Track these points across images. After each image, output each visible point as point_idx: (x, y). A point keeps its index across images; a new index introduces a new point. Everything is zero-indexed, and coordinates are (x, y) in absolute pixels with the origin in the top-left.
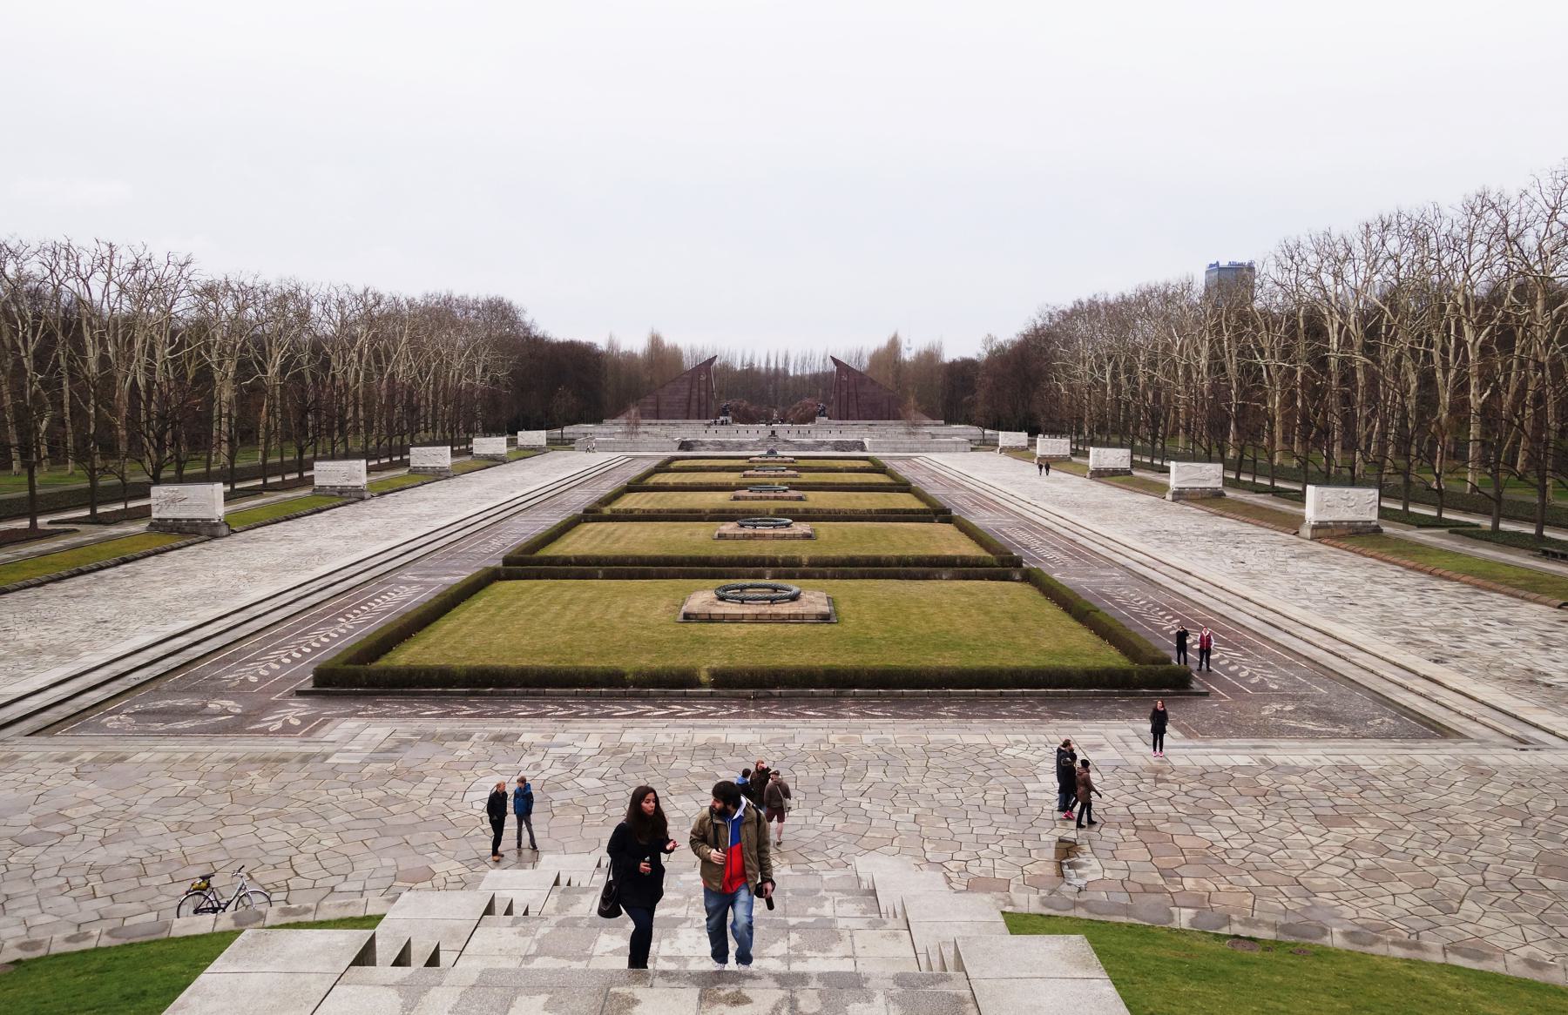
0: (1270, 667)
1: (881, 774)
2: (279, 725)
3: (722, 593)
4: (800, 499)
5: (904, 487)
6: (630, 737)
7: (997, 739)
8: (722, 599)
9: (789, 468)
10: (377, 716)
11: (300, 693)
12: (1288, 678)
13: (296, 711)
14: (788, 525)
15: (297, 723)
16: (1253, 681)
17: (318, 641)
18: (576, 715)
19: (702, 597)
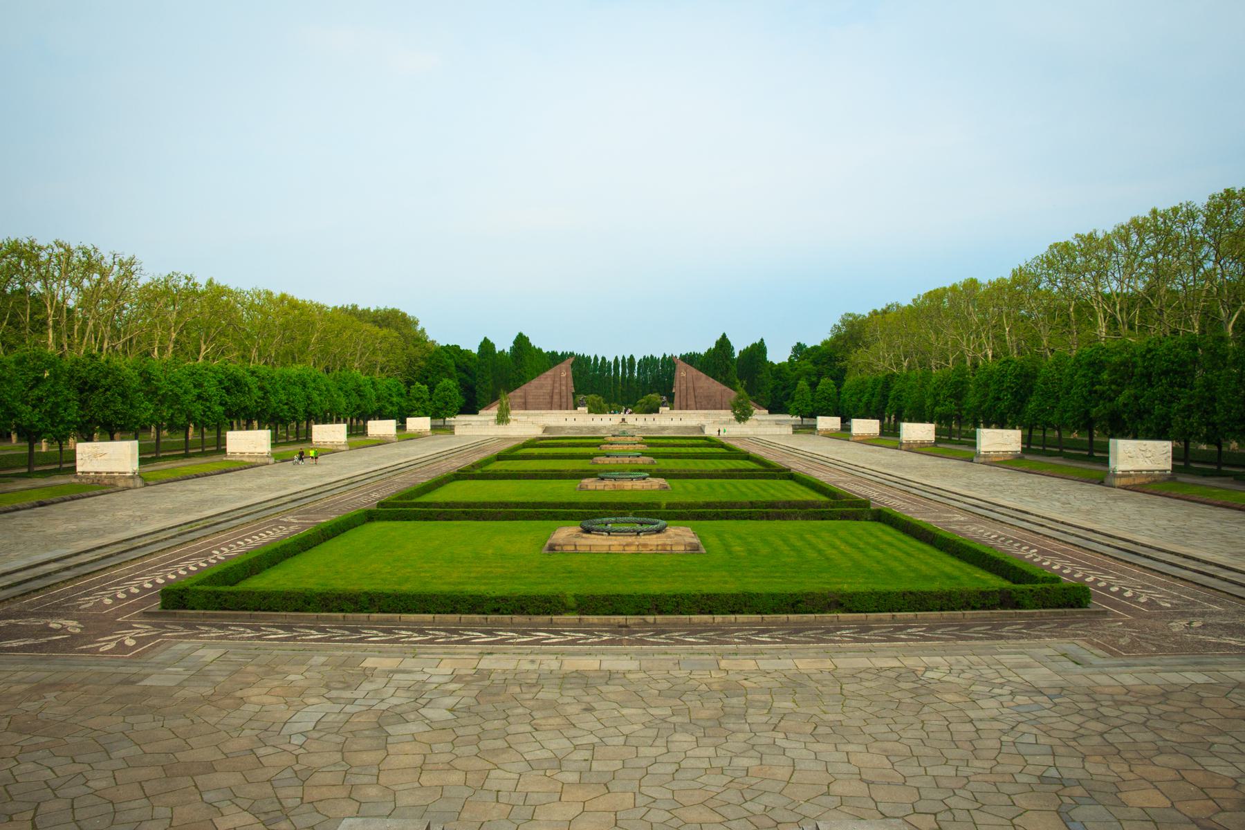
1: (792, 705)
7: (910, 662)
8: (588, 531)
12: (1174, 597)
19: (565, 533)
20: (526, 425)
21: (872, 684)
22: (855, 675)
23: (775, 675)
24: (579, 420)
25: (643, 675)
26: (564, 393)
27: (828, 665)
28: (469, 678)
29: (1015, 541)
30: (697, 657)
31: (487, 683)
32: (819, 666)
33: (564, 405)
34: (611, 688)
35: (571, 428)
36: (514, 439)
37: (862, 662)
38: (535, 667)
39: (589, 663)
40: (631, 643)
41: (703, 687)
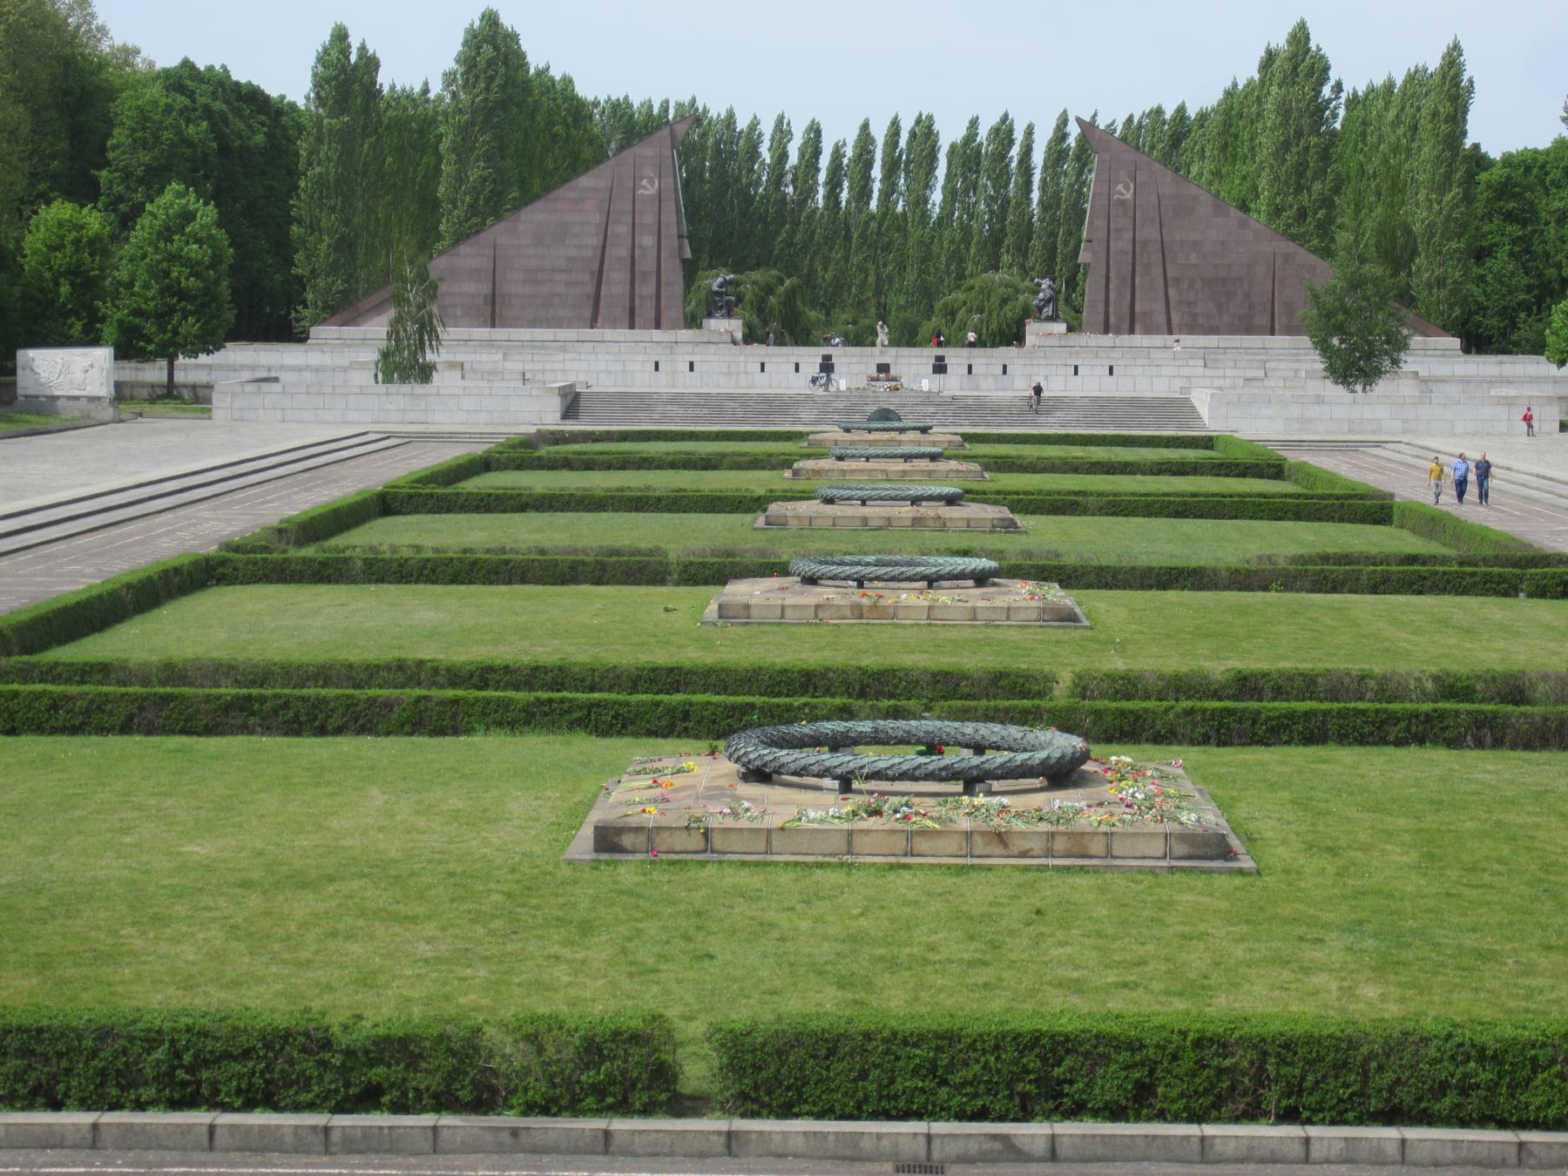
20: (494, 386)
24: (710, 370)
26: (647, 264)
33: (646, 310)
35: (677, 399)
36: (450, 437)
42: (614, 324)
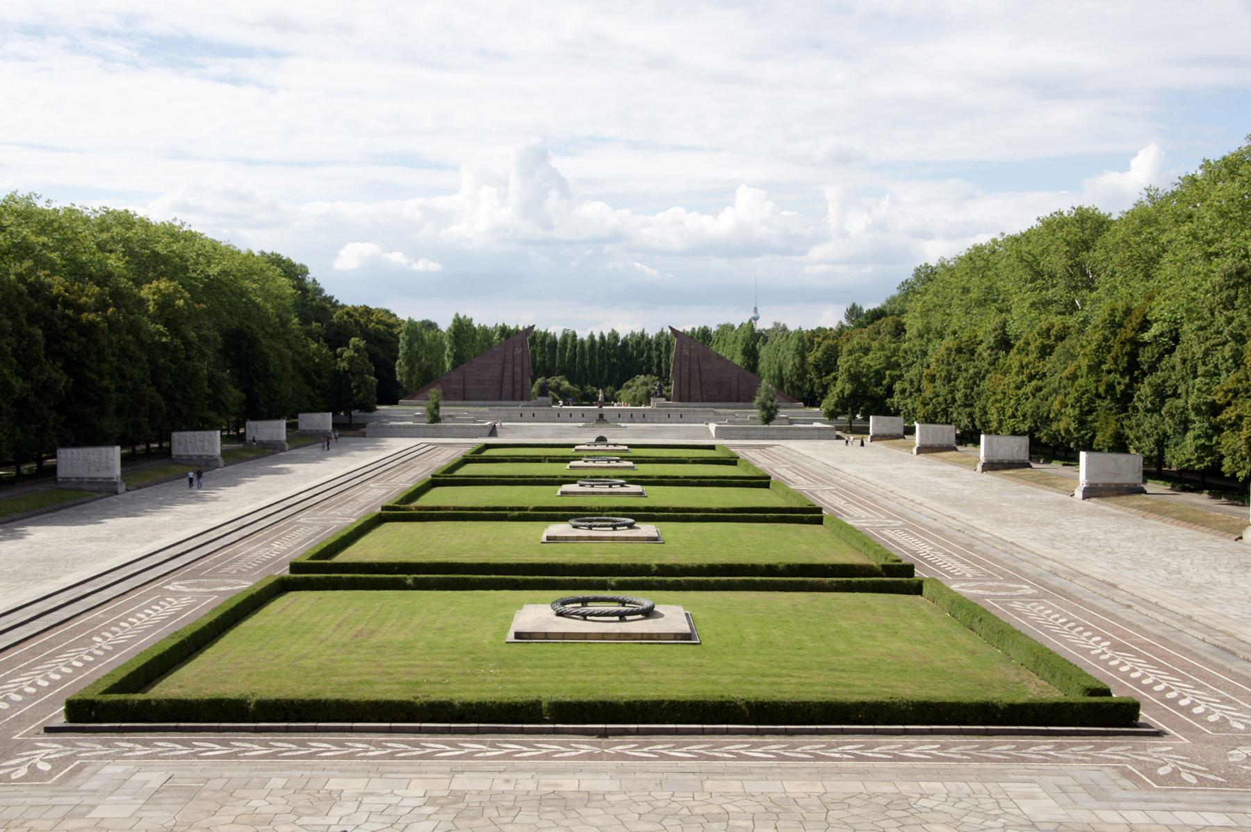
0: (1230, 702)
2: (23, 771)
3: (561, 609)
4: (640, 494)
5: (762, 482)
6: (461, 783)
7: (905, 788)
8: (560, 614)
9: (623, 458)
10: (146, 757)
11: (49, 730)
13: (53, 748)
14: (630, 526)
15: (46, 767)
16: (1212, 719)
17: (69, 665)
18: (392, 756)
21: (860, 811)
22: (844, 802)
23: (761, 798)
25: (624, 797)
26: (518, 378)
27: (819, 788)
28: (442, 801)
29: (1087, 628)
30: (681, 776)
31: (463, 805)
32: (809, 789)
34: (592, 811)
37: (855, 786)
38: (511, 787)
39: (568, 784)
40: (612, 757)
41: (685, 811)
42: (506, 399)
